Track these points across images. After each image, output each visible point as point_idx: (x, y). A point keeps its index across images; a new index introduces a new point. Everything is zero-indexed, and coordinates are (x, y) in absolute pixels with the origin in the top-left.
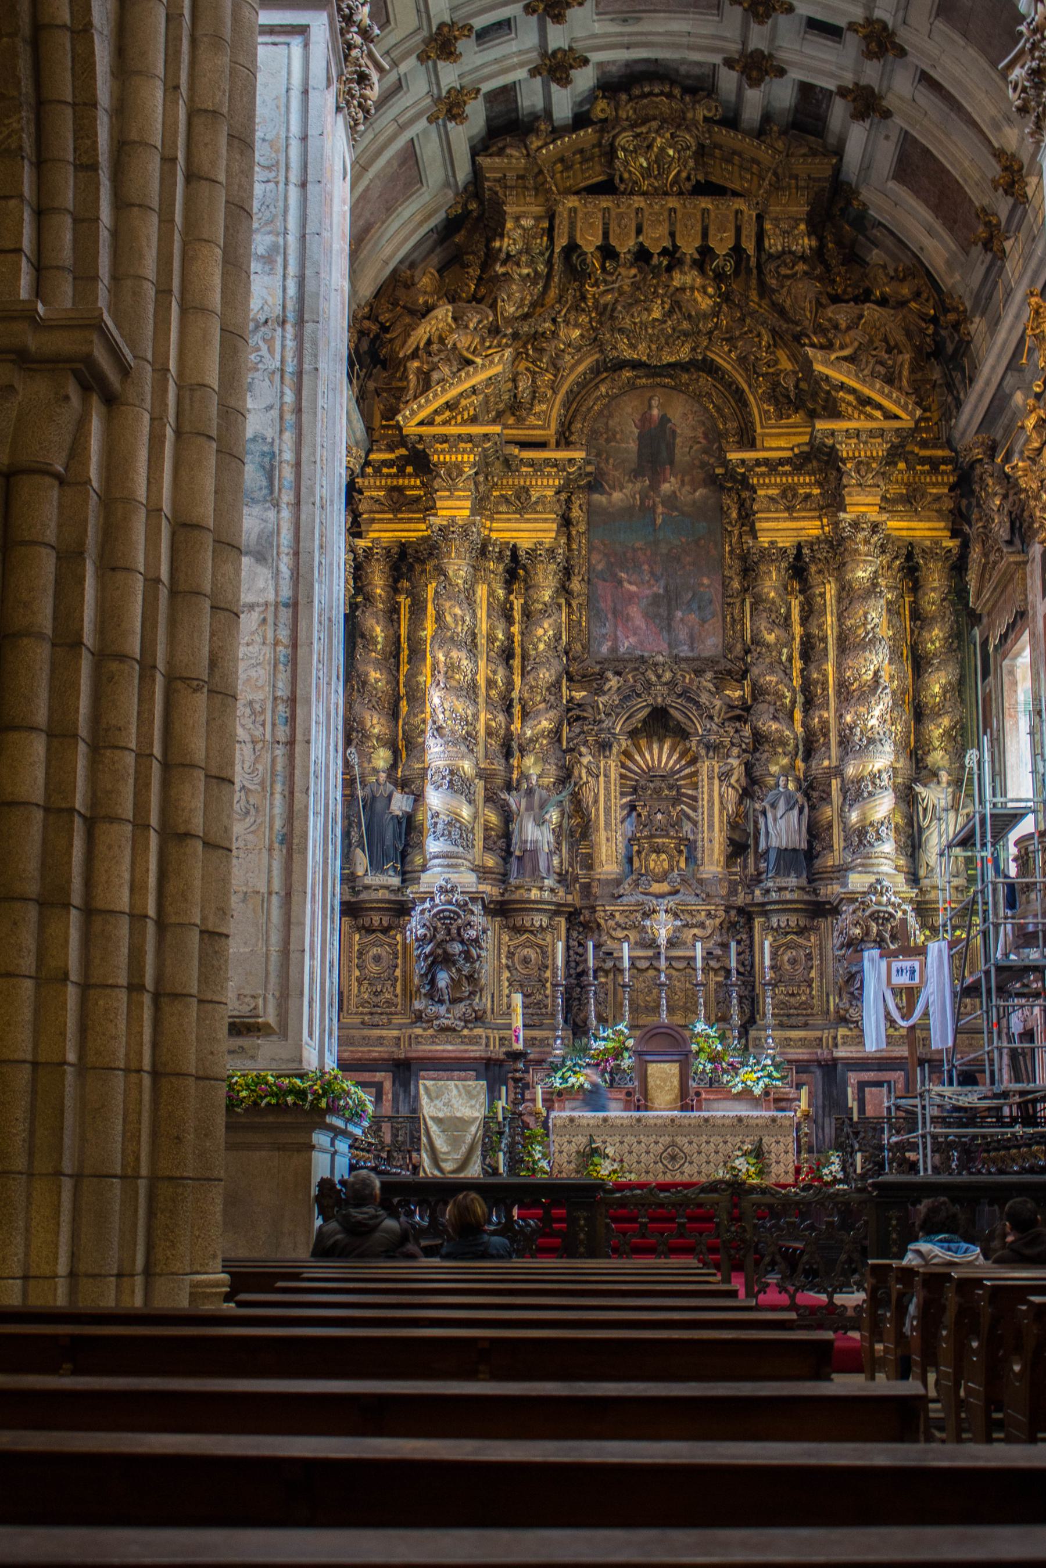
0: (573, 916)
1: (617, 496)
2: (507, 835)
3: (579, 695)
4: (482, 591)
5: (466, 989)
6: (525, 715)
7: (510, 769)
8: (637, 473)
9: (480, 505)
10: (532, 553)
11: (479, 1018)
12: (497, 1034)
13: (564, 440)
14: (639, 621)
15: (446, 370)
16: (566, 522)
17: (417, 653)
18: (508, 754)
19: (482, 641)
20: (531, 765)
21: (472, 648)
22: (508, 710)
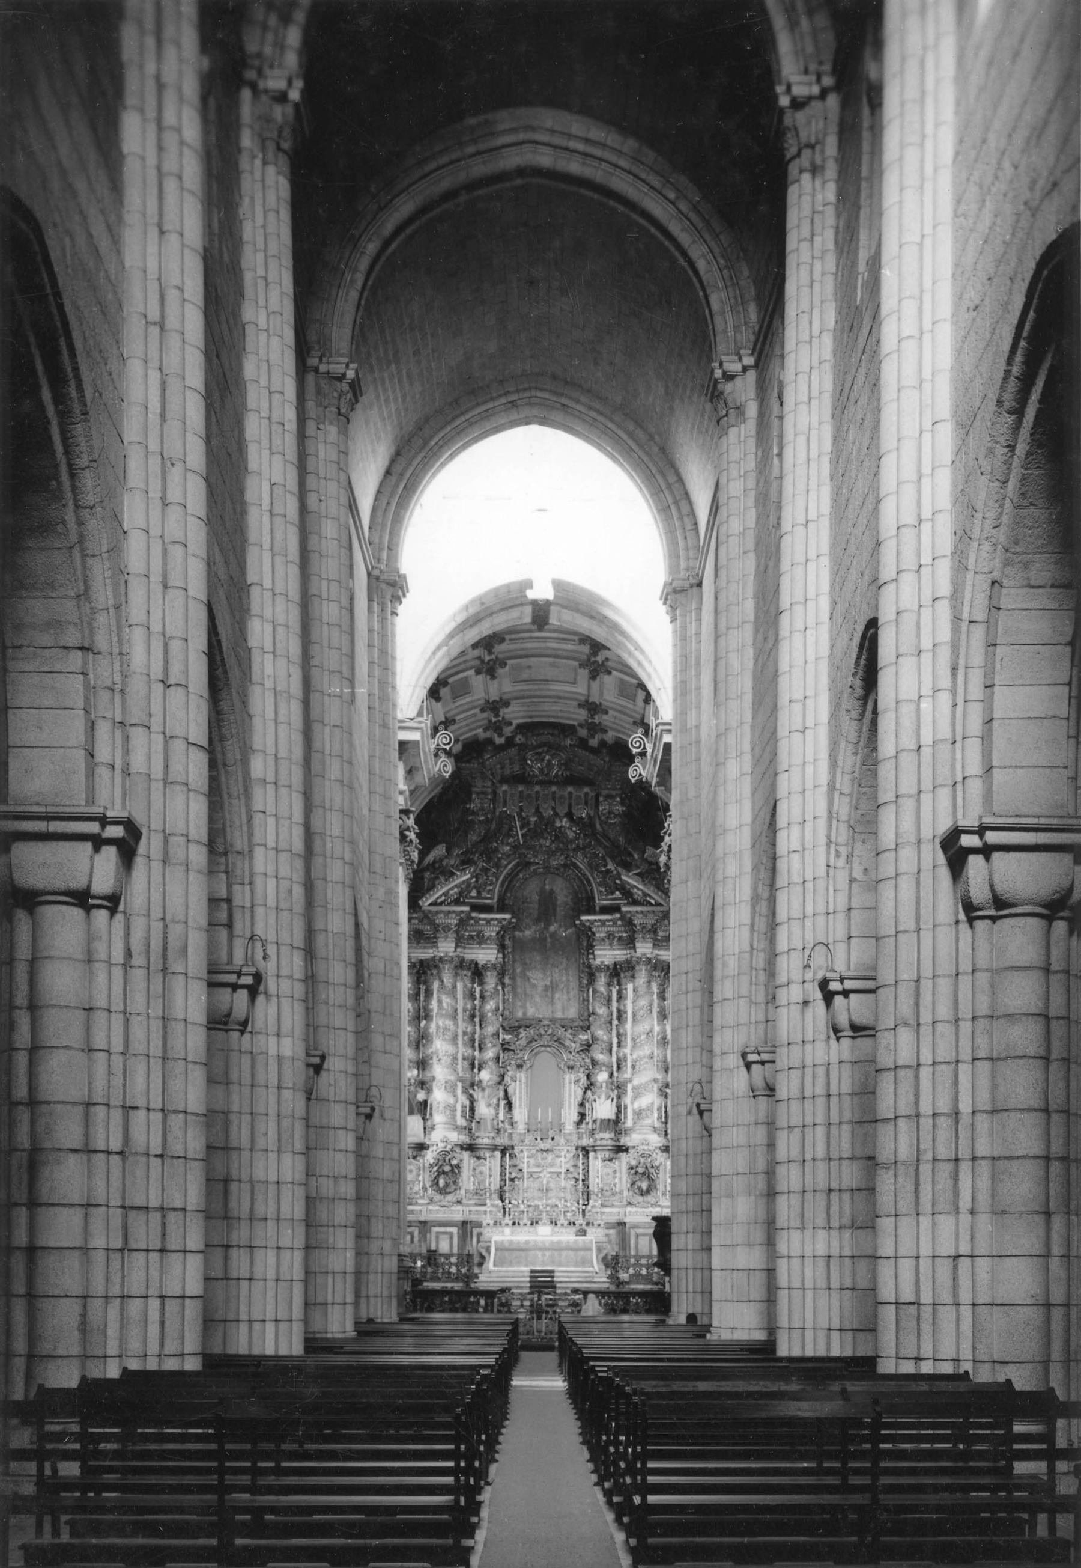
0: (503, 1152)
1: (527, 933)
2: (472, 1109)
3: (508, 1037)
4: (459, 985)
5: (453, 1187)
6: (481, 1049)
7: (473, 1077)
8: (538, 920)
9: (459, 941)
10: (485, 967)
11: (459, 1202)
12: (467, 1209)
13: (502, 908)
14: (538, 999)
15: (442, 879)
16: (502, 947)
17: (428, 1017)
18: (473, 1065)
19: (460, 1011)
20: (485, 1075)
21: (454, 1017)
22: (473, 1047)
